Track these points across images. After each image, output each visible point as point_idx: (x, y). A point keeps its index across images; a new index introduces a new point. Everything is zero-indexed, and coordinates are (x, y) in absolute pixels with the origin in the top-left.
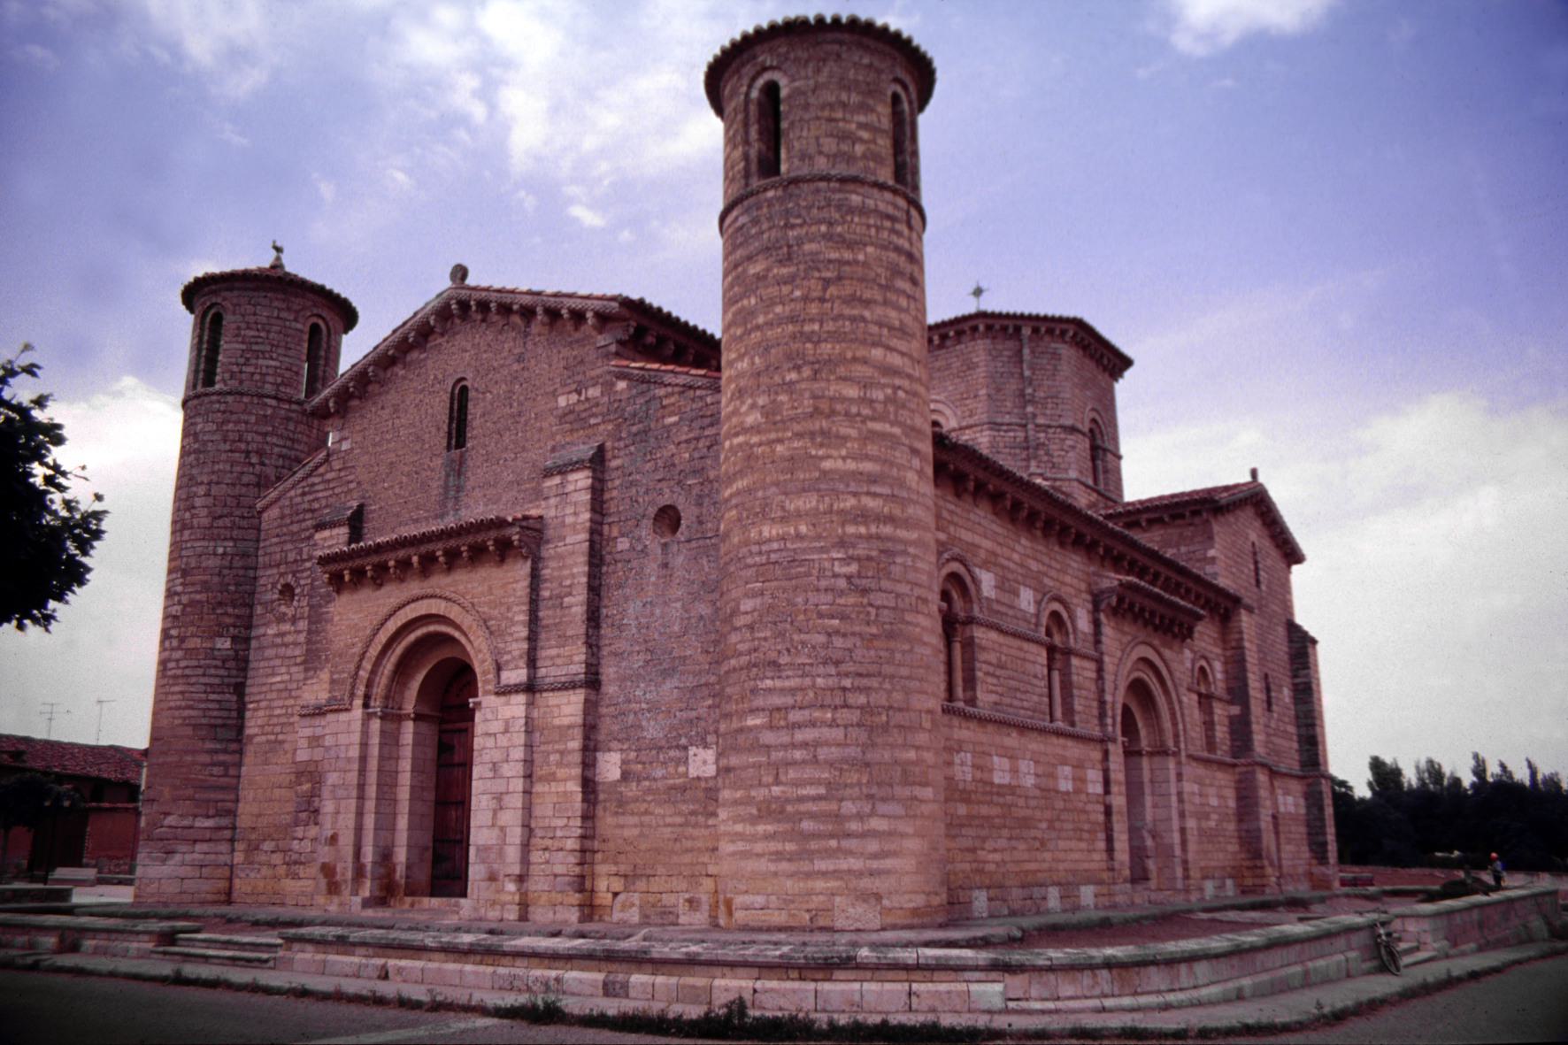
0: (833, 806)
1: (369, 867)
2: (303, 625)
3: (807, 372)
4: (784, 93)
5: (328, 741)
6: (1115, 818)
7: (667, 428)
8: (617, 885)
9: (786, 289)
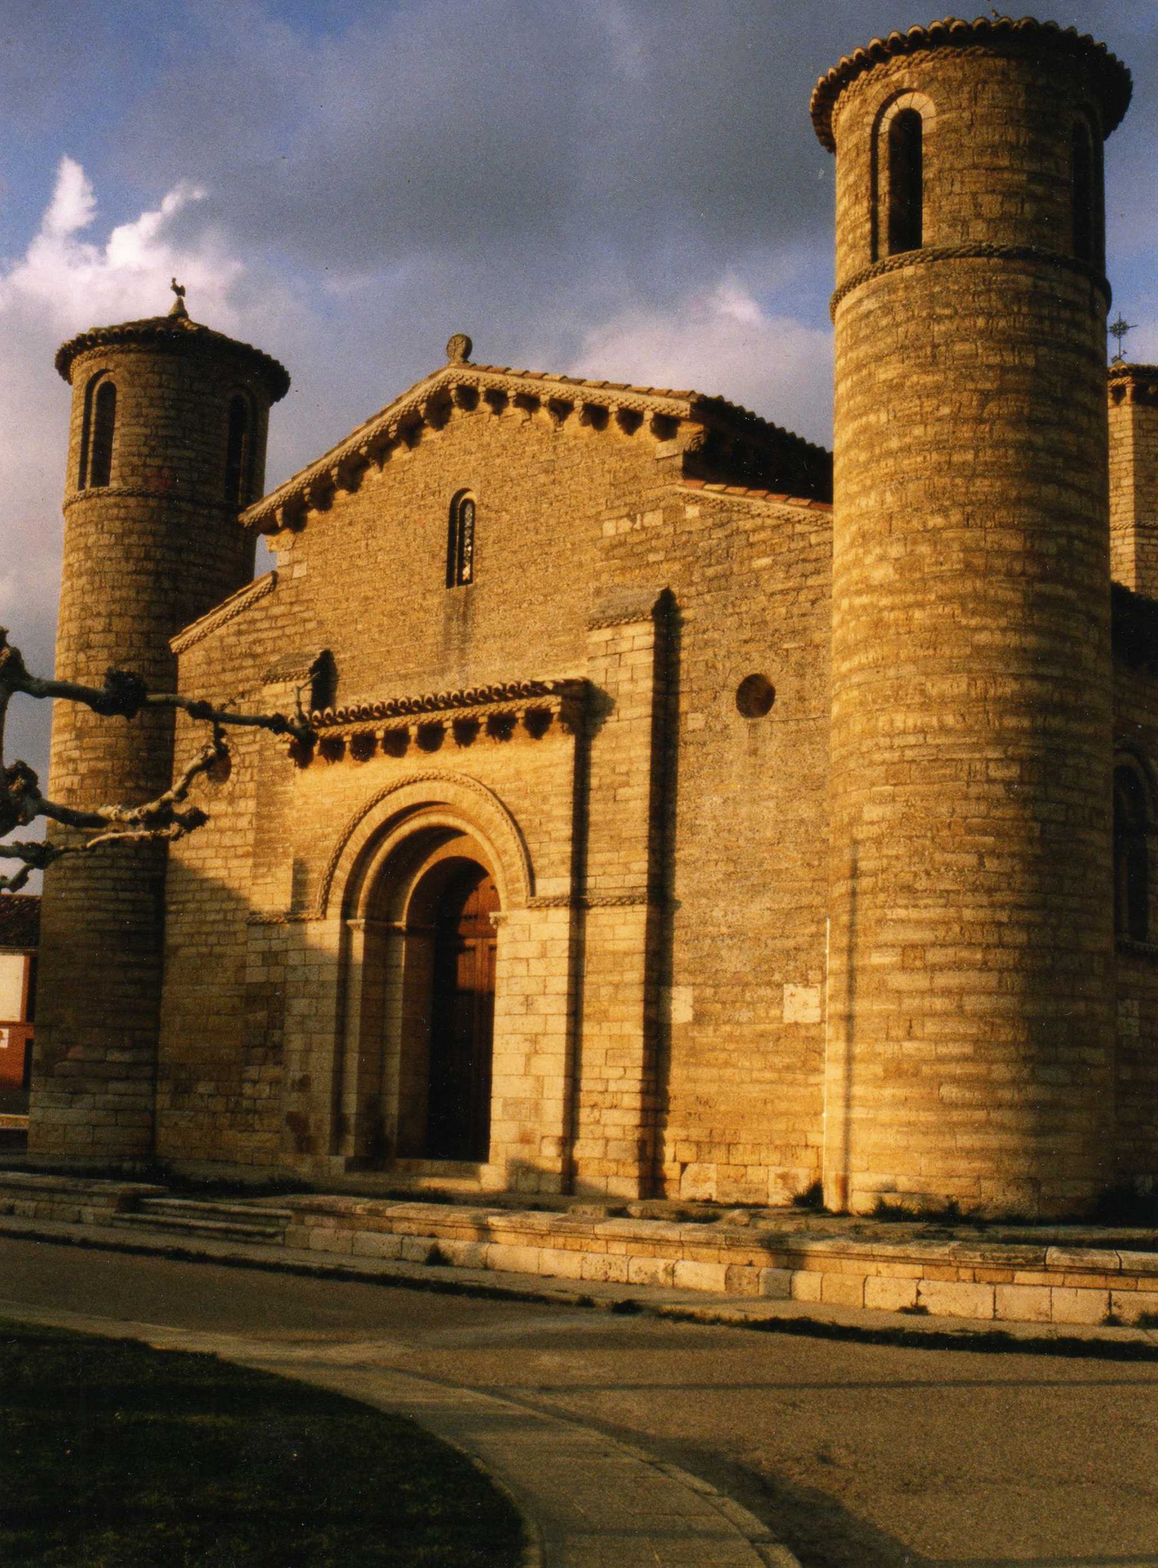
1: (352, 1120)
3: (956, 516)
4: (928, 127)
7: (757, 573)
8: (687, 1154)
9: (929, 404)
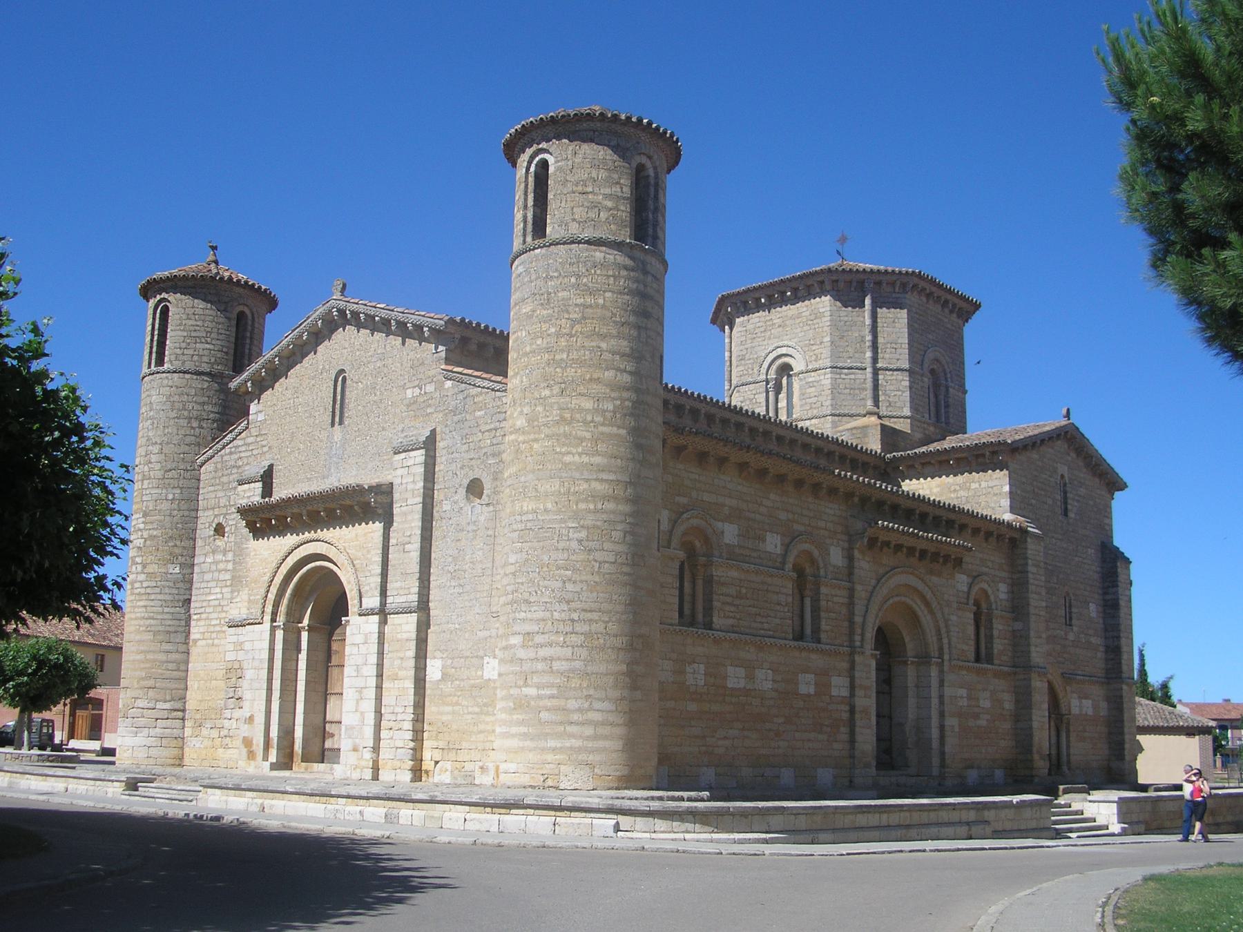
0: (562, 703)
2: (230, 556)
3: (556, 390)
4: (551, 170)
5: (247, 646)
6: (857, 716)
9: (545, 327)
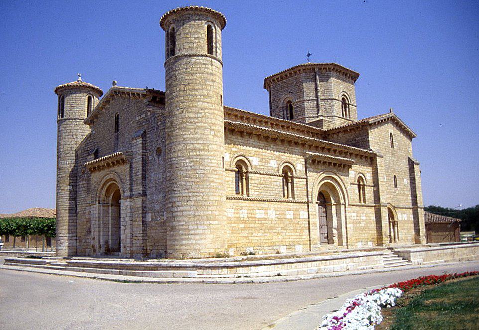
6: (311, 225)
8: (151, 249)
9: (175, 88)
